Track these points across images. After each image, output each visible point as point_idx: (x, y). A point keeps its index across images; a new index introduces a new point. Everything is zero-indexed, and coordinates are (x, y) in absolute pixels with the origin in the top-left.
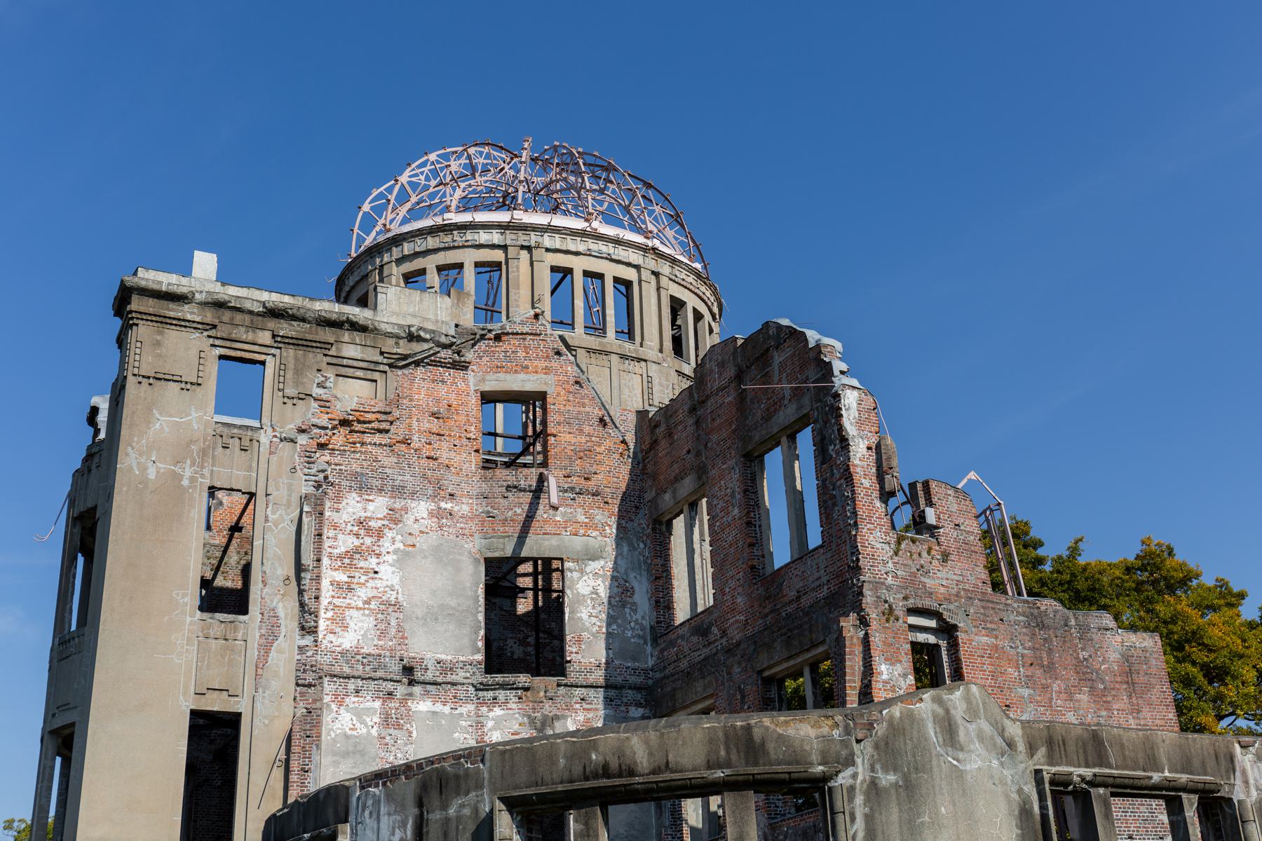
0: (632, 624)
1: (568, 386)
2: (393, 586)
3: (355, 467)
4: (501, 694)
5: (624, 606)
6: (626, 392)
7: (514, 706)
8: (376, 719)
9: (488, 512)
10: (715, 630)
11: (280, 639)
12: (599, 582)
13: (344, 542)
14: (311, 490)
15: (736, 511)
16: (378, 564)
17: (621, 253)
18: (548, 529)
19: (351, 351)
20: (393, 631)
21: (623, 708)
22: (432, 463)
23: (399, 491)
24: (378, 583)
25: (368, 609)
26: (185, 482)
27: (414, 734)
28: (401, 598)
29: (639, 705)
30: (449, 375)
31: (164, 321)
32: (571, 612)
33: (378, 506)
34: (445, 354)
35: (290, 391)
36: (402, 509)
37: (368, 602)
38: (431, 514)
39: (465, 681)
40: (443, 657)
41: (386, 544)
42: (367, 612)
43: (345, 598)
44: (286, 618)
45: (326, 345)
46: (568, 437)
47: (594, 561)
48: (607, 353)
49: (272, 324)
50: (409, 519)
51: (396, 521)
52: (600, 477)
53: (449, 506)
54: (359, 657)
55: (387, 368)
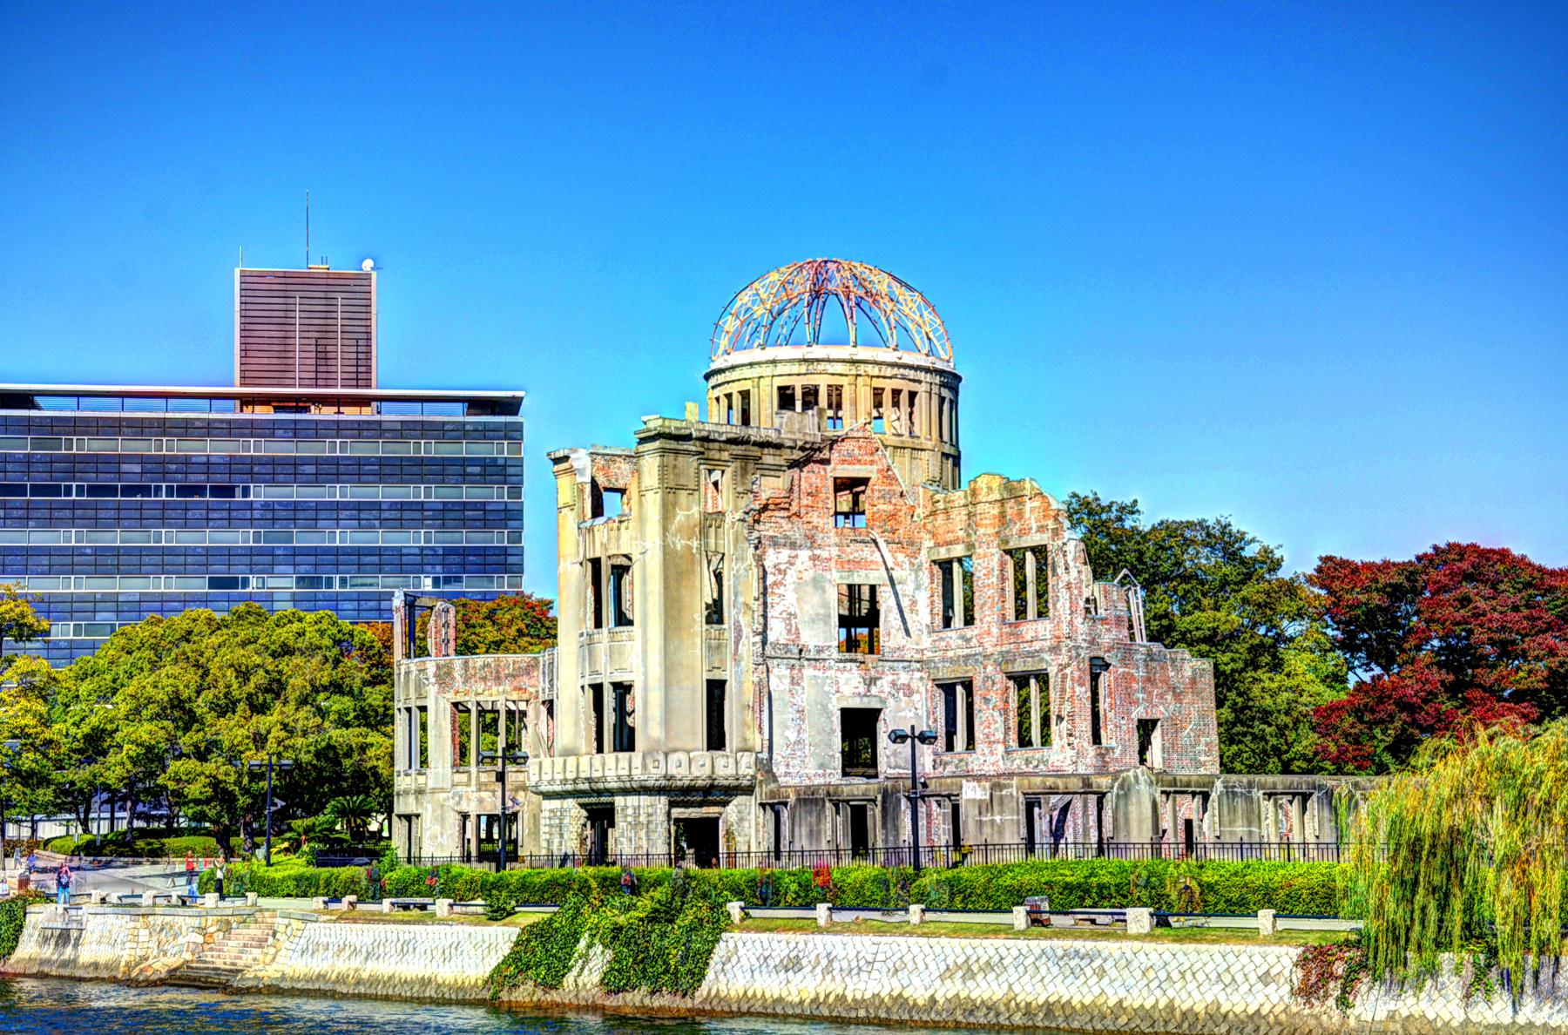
3: (771, 533)
4: (848, 665)
8: (788, 680)
10: (974, 640)
15: (994, 580)
22: (810, 526)
23: (793, 546)
26: (694, 551)
29: (918, 670)
31: (677, 452)
33: (785, 553)
35: (740, 489)
38: (810, 558)
49: (728, 446)
50: (798, 562)
51: (792, 564)
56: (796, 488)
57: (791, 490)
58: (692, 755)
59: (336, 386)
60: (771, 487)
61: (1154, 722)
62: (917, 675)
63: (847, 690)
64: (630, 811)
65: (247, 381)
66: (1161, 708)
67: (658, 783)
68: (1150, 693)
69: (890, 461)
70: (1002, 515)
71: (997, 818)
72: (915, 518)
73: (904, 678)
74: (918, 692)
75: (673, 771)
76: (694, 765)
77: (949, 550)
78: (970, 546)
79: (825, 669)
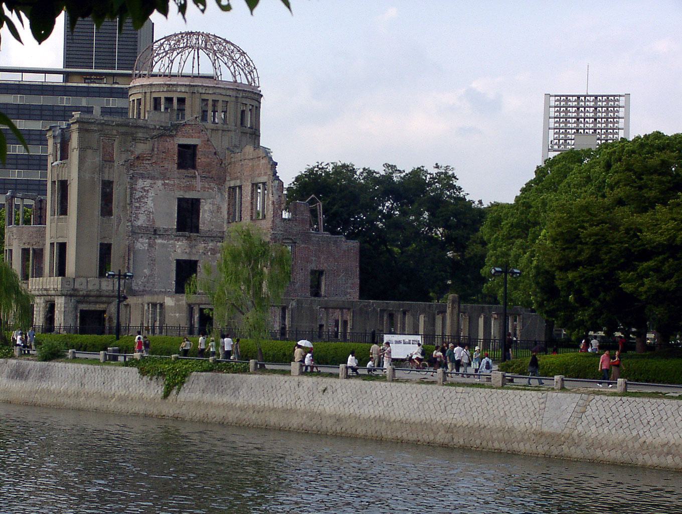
4: (181, 238)
5: (218, 212)
13: (138, 195)
14: (129, 180)
15: (249, 198)
17: (223, 92)
19: (140, 135)
20: (151, 220)
21: (216, 243)
22: (163, 169)
23: (153, 178)
24: (147, 206)
28: (154, 210)
30: (168, 140)
31: (87, 130)
32: (203, 215)
33: (148, 182)
34: (168, 133)
38: (163, 184)
41: (150, 194)
45: (132, 134)
46: (205, 160)
47: (209, 199)
48: (218, 130)
50: (155, 186)
55: (150, 139)
56: (156, 149)
57: (153, 150)
58: (88, 279)
59: (114, 68)
60: (141, 148)
61: (321, 273)
63: (179, 251)
64: (59, 305)
65: (70, 64)
66: (325, 265)
67: (68, 292)
68: (319, 258)
69: (210, 136)
70: (253, 166)
71: (177, 315)
73: (211, 245)
75: (77, 286)
76: (93, 284)
79: (168, 240)
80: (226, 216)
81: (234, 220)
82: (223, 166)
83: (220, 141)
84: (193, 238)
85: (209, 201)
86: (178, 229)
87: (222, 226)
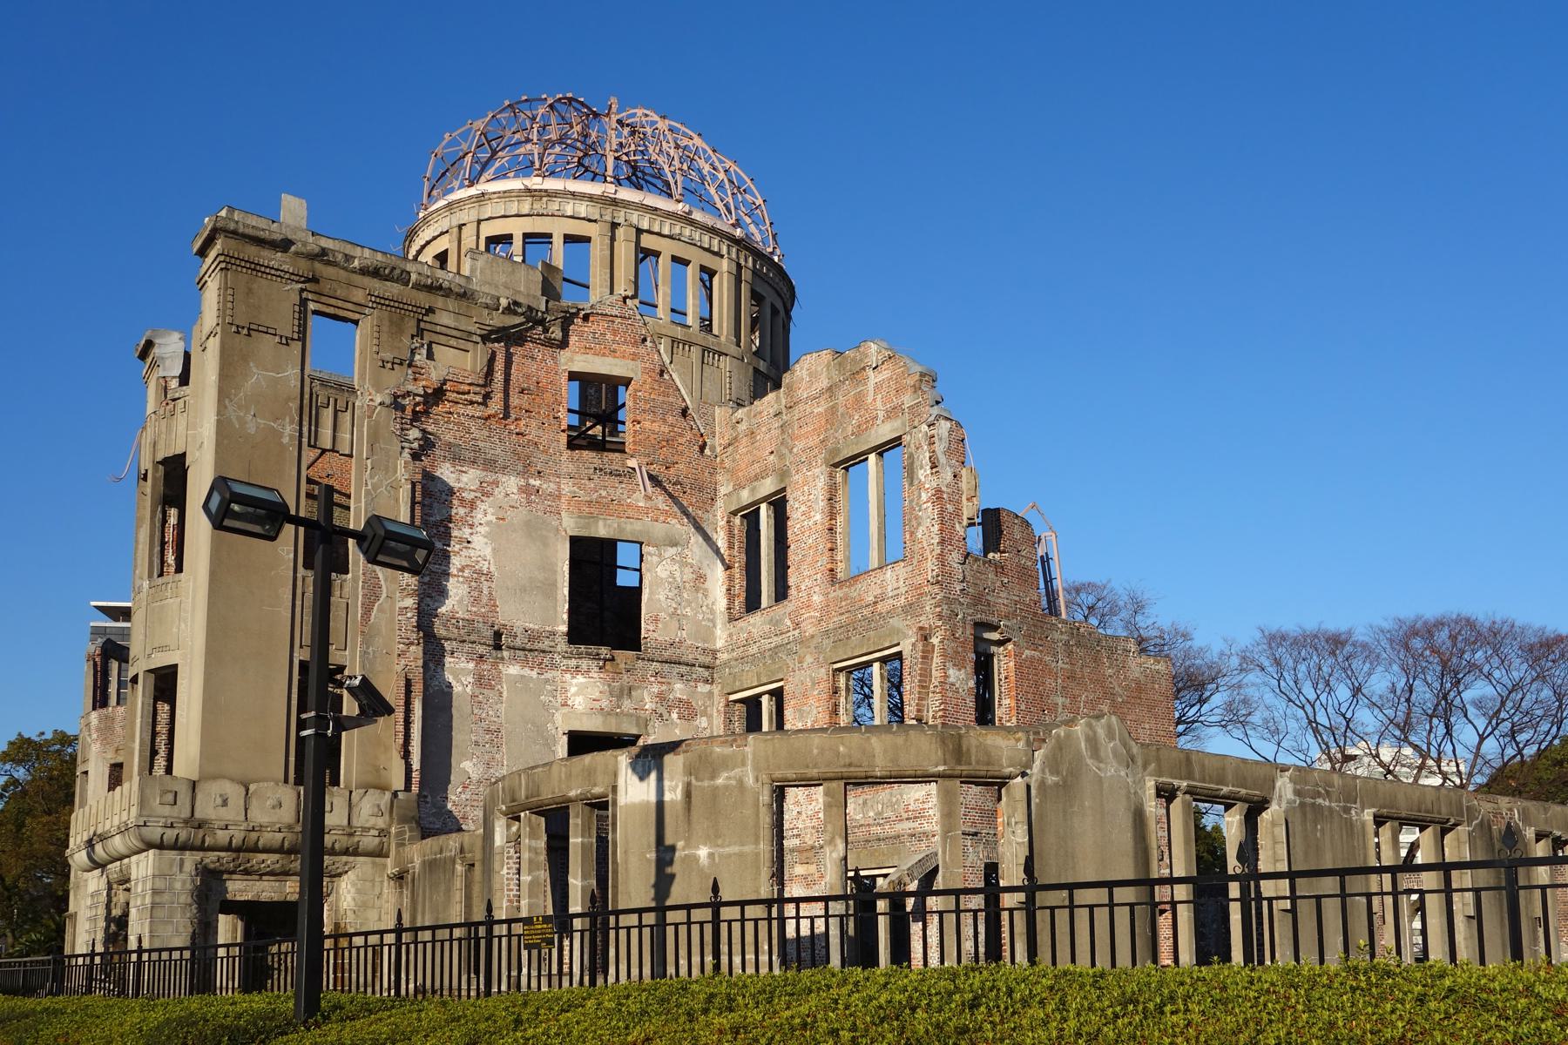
0: (704, 608)
1: (653, 375)
2: (485, 556)
4: (584, 664)
5: (697, 591)
6: (707, 384)
7: (595, 675)
9: (575, 492)
11: (381, 599)
12: (676, 567)
16: (472, 534)
18: (630, 513)
20: (485, 600)
23: (490, 465)
24: (472, 553)
25: (462, 576)
27: (505, 694)
28: (491, 570)
29: (707, 681)
30: (539, 352)
32: (651, 593)
36: (493, 483)
37: (462, 570)
38: (522, 490)
39: (552, 649)
40: (531, 626)
41: (479, 516)
42: (461, 579)
43: (440, 565)
44: (386, 580)
50: (499, 492)
51: (488, 494)
52: (681, 466)
53: (537, 483)
54: (454, 621)
62: (703, 688)
63: (579, 703)
69: (667, 360)
72: (707, 451)
74: (704, 714)
77: (753, 490)
78: (783, 474)
80: (722, 603)
81: (752, 604)
82: (709, 453)
83: (696, 375)
84: (622, 666)
85: (672, 551)
86: (576, 635)
87: (709, 634)
